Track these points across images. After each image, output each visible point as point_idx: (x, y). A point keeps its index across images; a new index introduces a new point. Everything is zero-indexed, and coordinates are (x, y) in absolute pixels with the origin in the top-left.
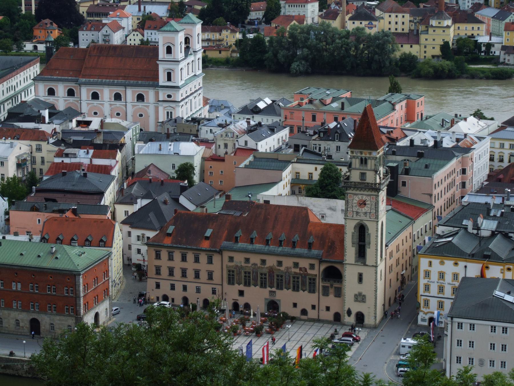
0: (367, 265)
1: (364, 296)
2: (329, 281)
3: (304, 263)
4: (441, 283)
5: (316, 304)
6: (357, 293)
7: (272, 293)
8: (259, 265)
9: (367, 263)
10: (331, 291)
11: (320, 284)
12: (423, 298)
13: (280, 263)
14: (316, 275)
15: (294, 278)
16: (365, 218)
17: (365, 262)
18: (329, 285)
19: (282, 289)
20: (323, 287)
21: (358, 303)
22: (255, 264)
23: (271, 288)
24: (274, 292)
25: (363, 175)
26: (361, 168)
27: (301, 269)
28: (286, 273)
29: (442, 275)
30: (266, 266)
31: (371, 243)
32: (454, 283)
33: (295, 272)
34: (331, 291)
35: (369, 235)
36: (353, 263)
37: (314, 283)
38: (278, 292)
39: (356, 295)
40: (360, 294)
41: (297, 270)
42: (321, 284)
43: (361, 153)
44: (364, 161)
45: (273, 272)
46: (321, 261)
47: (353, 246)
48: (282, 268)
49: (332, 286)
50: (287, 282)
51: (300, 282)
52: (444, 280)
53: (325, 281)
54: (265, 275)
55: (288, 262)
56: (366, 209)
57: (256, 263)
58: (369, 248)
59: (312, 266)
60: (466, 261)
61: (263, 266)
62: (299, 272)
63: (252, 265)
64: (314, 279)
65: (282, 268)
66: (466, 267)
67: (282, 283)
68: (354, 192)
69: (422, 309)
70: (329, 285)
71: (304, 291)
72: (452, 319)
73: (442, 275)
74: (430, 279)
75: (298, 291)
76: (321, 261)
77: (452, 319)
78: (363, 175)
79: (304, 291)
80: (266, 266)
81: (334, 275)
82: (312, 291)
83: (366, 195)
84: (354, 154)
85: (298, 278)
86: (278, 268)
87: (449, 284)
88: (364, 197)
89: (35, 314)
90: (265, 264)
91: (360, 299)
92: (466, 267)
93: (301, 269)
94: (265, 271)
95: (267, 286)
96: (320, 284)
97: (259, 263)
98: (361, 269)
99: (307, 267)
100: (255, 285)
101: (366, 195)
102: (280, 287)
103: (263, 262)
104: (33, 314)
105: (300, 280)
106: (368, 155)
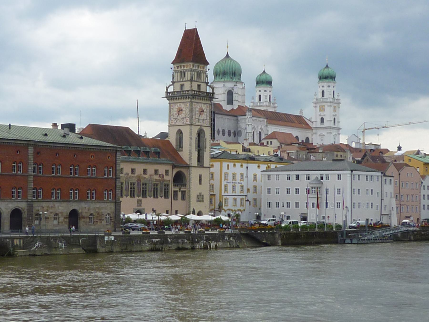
0: (205, 167)
1: (203, 196)
2: (178, 186)
3: (162, 169)
4: (234, 183)
5: (169, 209)
6: (198, 194)
7: (139, 201)
8: (130, 174)
9: (204, 166)
10: (180, 194)
11: (172, 188)
12: (224, 197)
13: (145, 171)
14: (170, 181)
15: (154, 185)
16: (203, 124)
17: (203, 165)
18: (178, 189)
19: (146, 197)
20: (174, 191)
21: (199, 203)
22: (127, 174)
23: (139, 197)
24: (141, 201)
25: (199, 86)
26: (198, 80)
27: (160, 176)
28: (149, 180)
29: (234, 175)
30: (135, 175)
31: (207, 147)
32: (241, 182)
33: (156, 179)
34: (180, 194)
35: (206, 139)
36: (196, 165)
37: (168, 189)
38: (144, 200)
39: (198, 196)
40: (200, 194)
41: (157, 177)
42: (173, 189)
43: (198, 67)
44: (199, 75)
45: (140, 181)
46: (174, 167)
47: (196, 151)
48: (147, 176)
49: (180, 190)
50: (150, 190)
51: (158, 190)
52: (236, 180)
53: (175, 186)
54: (134, 184)
55: (151, 169)
56: (203, 116)
57: (128, 172)
58: (206, 151)
59: (167, 172)
60: (248, 163)
61: (133, 175)
62: (158, 179)
63: (125, 174)
64: (168, 185)
65: (147, 176)
66: (247, 167)
67: (146, 191)
68: (197, 101)
69: (224, 207)
70: (178, 189)
71: (161, 197)
72: (352, 172)
73: (234, 175)
74: (228, 180)
75: (157, 197)
76: (174, 167)
77: (352, 172)
78: (199, 86)
79: (161, 197)
80: (135, 175)
81: (180, 179)
82: (166, 196)
83: (204, 103)
84: (194, 68)
85: (157, 185)
86: (144, 176)
87: (238, 183)
88: (203, 105)
89: (76, 204)
90: (134, 174)
91: (200, 199)
92: (247, 167)
93: (160, 175)
94: (134, 180)
95: (136, 195)
96: (172, 188)
97: (130, 172)
98: (201, 171)
99: (164, 174)
100: (127, 196)
101: (204, 103)
102: (144, 195)
103: (133, 171)
104: (73, 204)
105: (159, 186)
106: (202, 69)
